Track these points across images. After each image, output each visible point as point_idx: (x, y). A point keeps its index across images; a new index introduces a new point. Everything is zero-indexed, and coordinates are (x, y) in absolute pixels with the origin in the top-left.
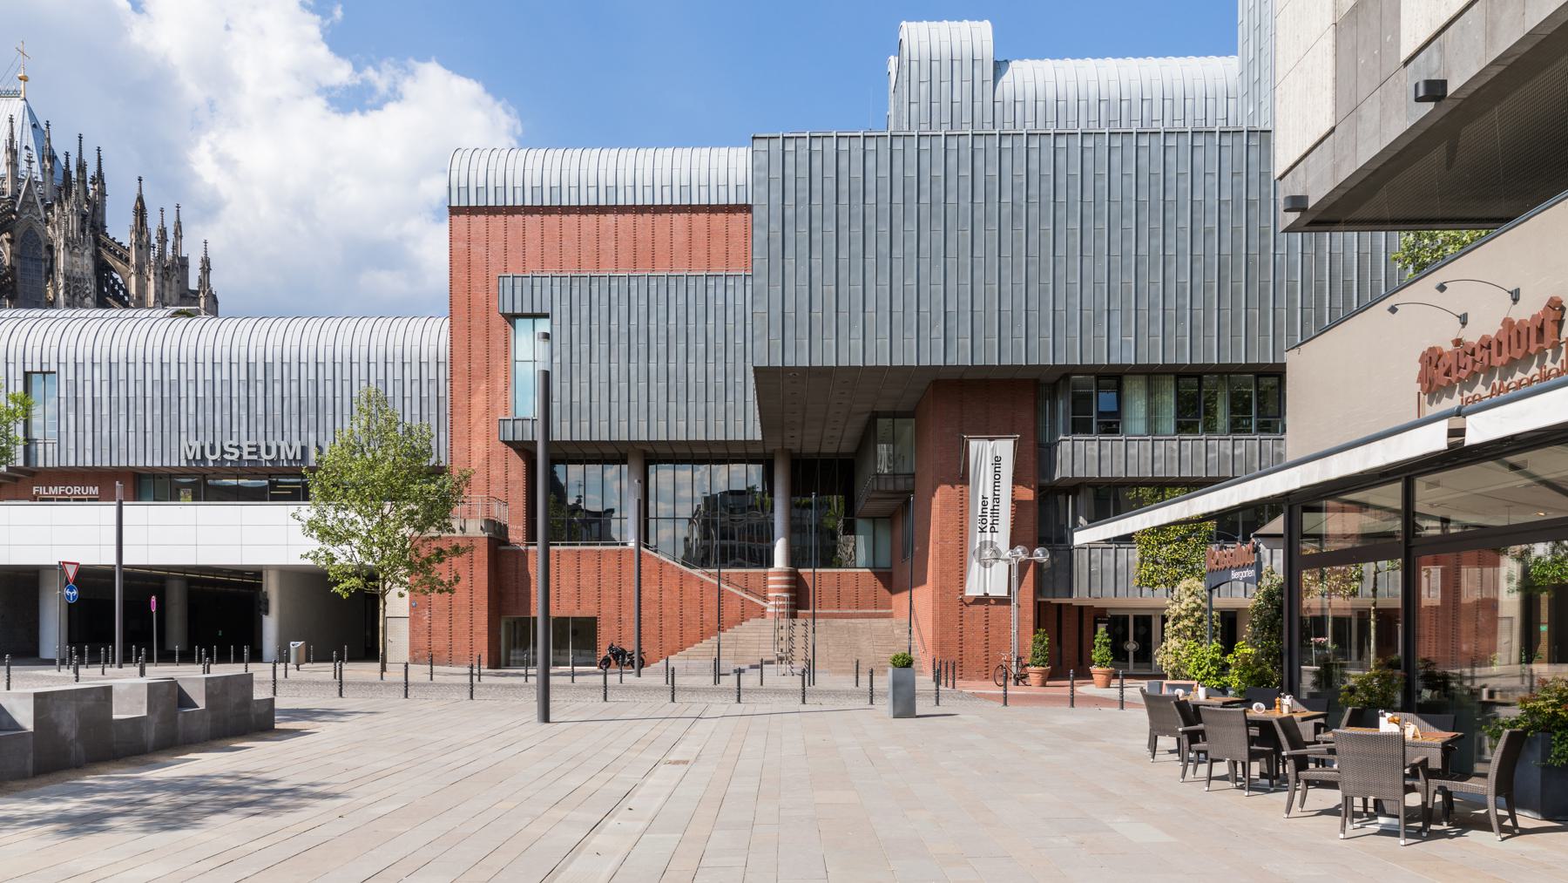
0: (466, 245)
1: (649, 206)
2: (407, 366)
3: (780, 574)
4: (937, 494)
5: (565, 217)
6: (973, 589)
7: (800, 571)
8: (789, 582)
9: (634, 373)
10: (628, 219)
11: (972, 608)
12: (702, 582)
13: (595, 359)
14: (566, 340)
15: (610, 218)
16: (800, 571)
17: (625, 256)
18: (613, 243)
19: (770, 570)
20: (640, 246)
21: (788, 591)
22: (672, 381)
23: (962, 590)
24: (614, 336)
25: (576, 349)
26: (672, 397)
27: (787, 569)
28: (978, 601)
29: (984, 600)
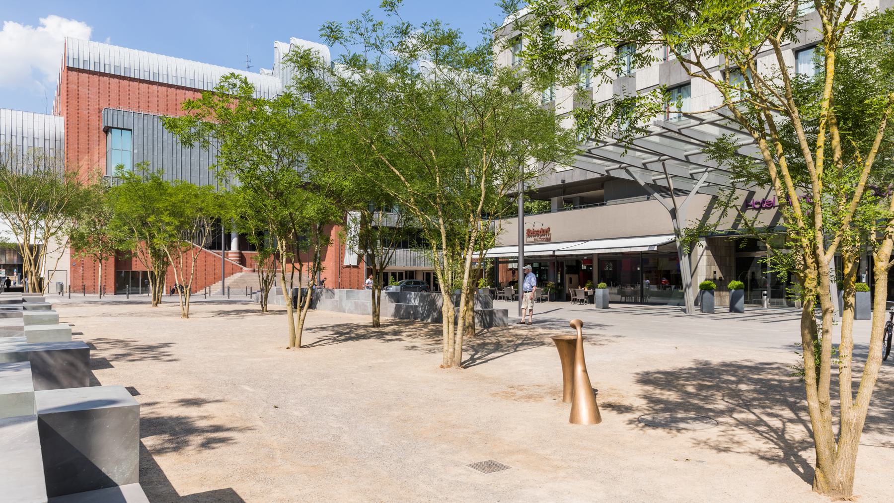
0: (76, 87)
1: (175, 85)
2: (25, 139)
3: (235, 253)
4: (334, 228)
5: (131, 82)
6: (346, 263)
7: (243, 252)
8: (239, 257)
9: (174, 161)
10: (164, 89)
11: (345, 269)
12: (215, 256)
13: (155, 153)
14: (141, 143)
15: (155, 87)
16: (243, 252)
17: (162, 105)
18: (156, 100)
19: (229, 251)
20: (170, 102)
21: (239, 260)
22: (193, 167)
23: (342, 263)
24: (165, 144)
25: (145, 148)
26: (193, 174)
27: (238, 251)
28: (347, 267)
29: (349, 267)
